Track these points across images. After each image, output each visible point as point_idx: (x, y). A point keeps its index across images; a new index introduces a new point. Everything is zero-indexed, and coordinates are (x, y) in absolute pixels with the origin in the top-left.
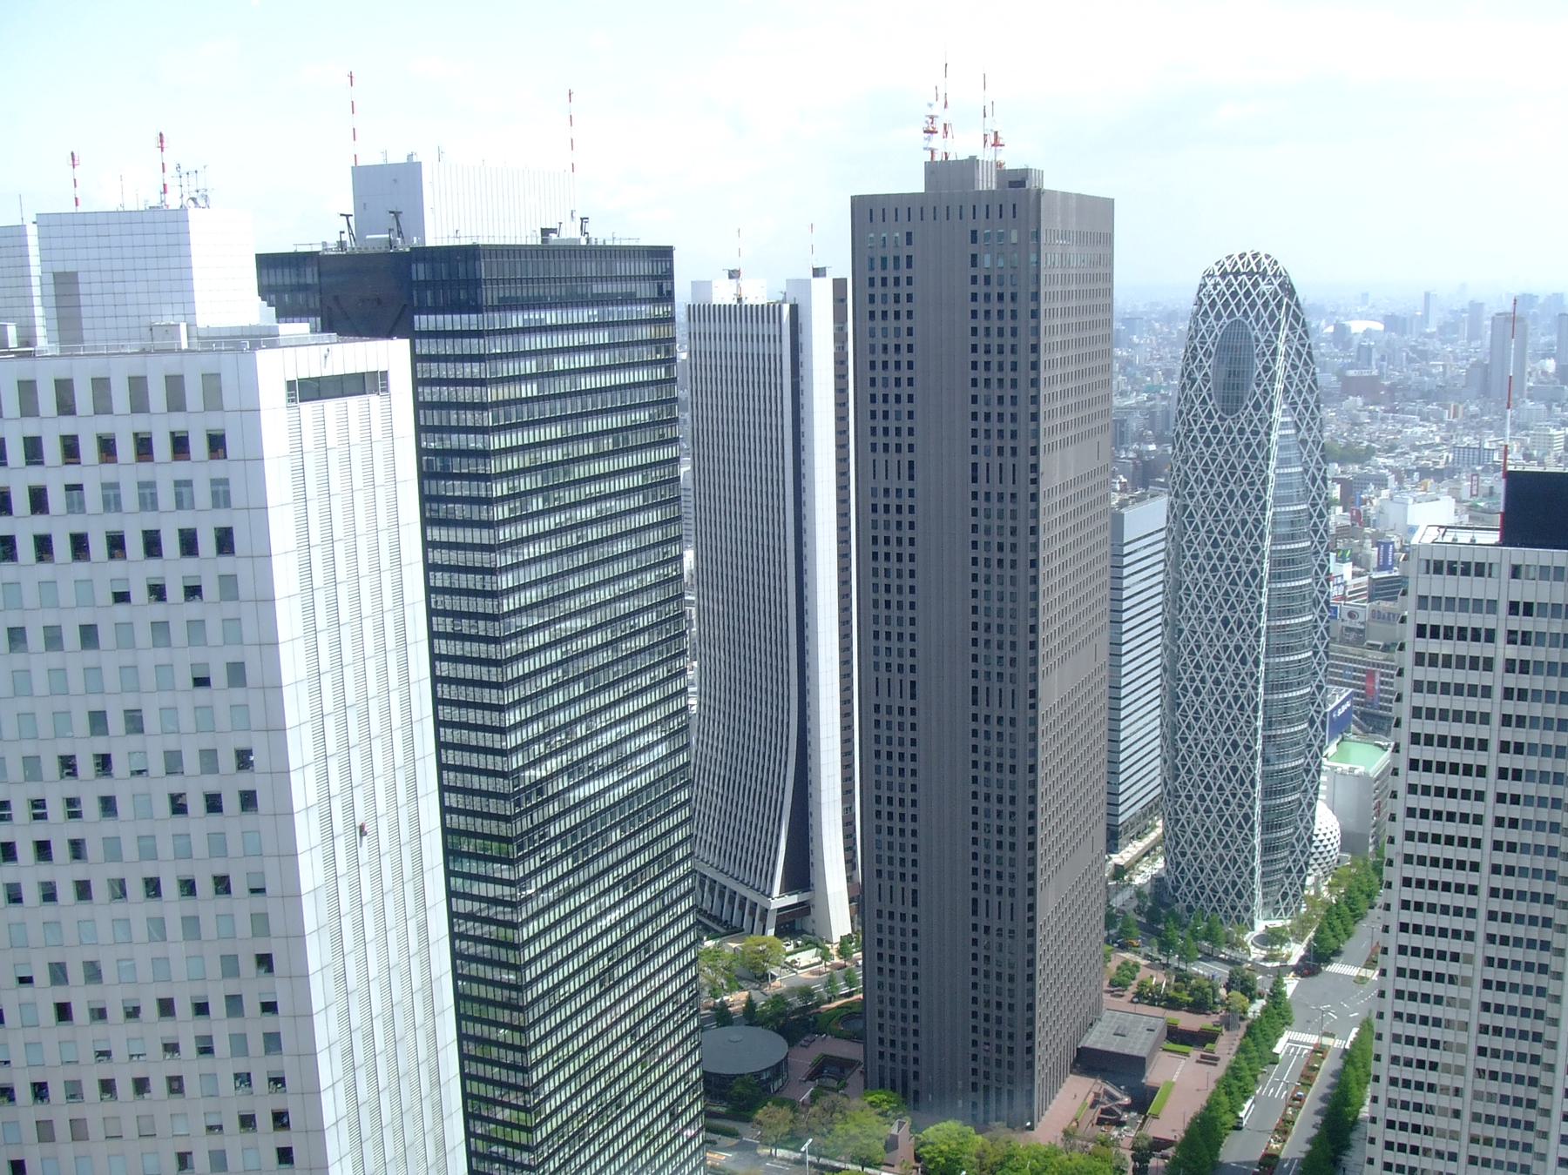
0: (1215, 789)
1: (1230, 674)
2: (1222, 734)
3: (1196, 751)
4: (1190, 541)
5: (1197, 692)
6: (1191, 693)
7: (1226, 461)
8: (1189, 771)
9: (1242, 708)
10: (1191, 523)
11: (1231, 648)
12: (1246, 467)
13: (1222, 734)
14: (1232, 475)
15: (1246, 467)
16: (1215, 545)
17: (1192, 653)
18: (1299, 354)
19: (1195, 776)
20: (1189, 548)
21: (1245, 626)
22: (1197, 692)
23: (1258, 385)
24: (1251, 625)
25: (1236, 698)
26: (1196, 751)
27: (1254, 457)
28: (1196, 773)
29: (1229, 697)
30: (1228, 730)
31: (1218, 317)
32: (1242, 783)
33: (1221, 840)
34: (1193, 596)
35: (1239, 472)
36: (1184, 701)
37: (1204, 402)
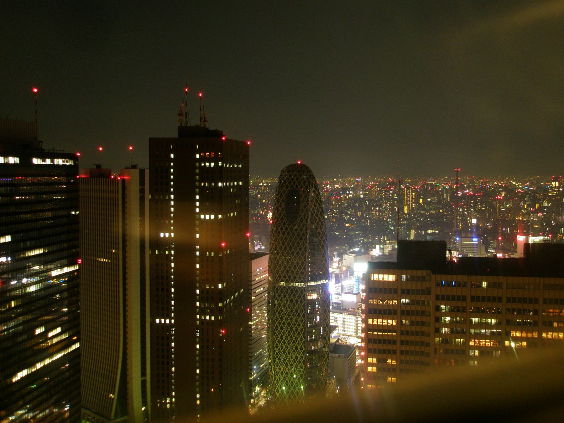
0: (289, 365)
1: (294, 321)
2: (291, 344)
3: (282, 351)
4: (278, 271)
5: (282, 328)
6: (279, 329)
7: (291, 241)
8: (279, 359)
9: (299, 334)
10: (278, 264)
11: (294, 311)
12: (298, 243)
13: (291, 344)
14: (293, 245)
15: (298, 243)
16: (287, 272)
17: (279, 313)
18: (317, 201)
19: (282, 361)
20: (277, 273)
21: (299, 302)
22: (282, 328)
23: (302, 212)
24: (301, 302)
25: (297, 330)
26: (282, 351)
27: (301, 239)
28: (282, 359)
29: (294, 329)
30: (294, 342)
31: (287, 187)
32: (300, 362)
33: (292, 386)
34: (279, 291)
35: (296, 245)
36: (277, 332)
37: (282, 218)
